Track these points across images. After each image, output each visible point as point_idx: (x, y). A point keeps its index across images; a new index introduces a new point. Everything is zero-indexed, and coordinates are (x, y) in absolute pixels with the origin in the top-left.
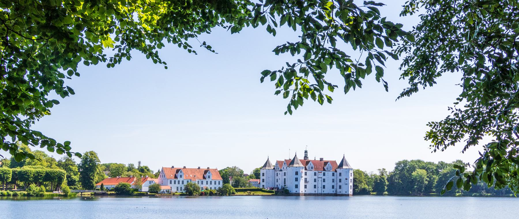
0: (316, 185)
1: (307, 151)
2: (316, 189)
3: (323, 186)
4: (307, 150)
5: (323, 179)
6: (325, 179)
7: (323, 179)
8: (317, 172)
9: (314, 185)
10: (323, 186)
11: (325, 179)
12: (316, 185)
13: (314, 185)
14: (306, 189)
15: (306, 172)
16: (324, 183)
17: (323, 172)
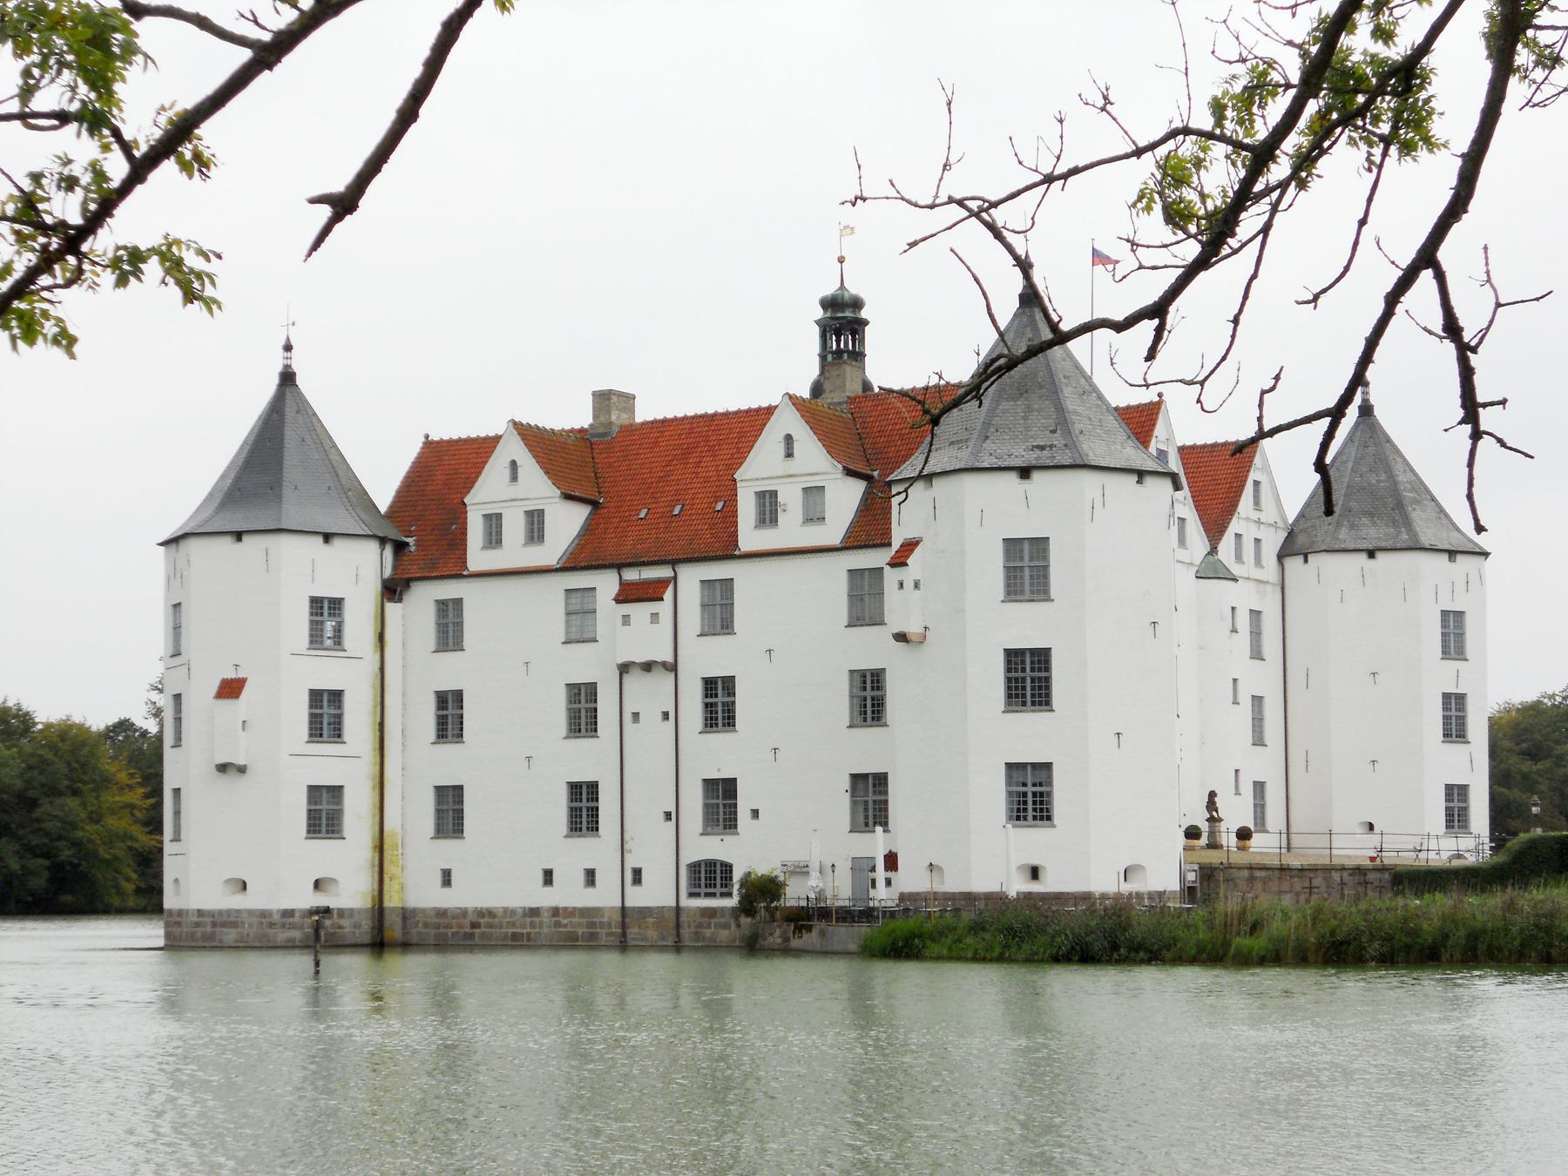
0: (593, 787)
1: (857, 304)
2: (599, 850)
3: (710, 785)
4: (854, 288)
5: (710, 685)
6: (729, 683)
7: (710, 685)
8: (606, 584)
9: (575, 789)
10: (710, 785)
11: (729, 683)
12: (593, 787)
13: (575, 789)
14: (448, 852)
15: (458, 602)
16: (719, 739)
17: (691, 579)
